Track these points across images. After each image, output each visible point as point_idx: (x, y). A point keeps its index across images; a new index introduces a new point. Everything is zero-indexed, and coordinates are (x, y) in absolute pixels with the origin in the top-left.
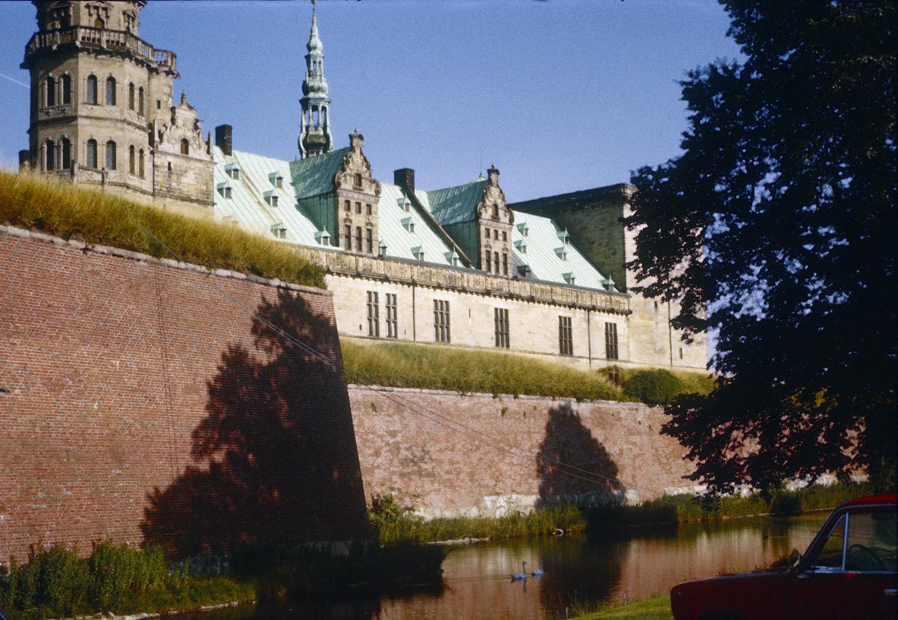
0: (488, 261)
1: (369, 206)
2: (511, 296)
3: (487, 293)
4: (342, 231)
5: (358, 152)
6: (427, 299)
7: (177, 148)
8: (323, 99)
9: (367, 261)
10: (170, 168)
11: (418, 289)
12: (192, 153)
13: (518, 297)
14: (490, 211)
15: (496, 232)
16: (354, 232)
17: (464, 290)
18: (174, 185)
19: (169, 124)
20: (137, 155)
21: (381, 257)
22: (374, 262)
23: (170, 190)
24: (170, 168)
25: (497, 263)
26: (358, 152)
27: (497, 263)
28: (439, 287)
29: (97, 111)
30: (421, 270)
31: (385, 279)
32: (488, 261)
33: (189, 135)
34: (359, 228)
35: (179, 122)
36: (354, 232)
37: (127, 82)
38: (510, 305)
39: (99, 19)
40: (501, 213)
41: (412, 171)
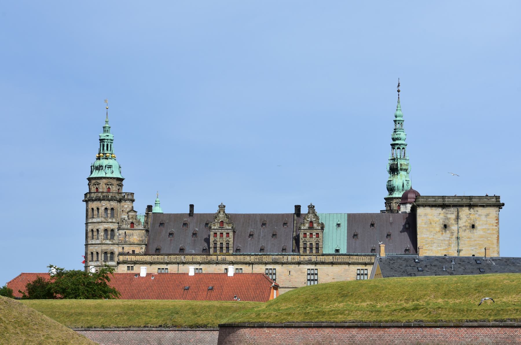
0: (305, 248)
1: (228, 234)
2: (316, 263)
3: (299, 263)
4: (212, 245)
5: (222, 212)
6: (261, 269)
7: (129, 226)
8: (397, 144)
9: (223, 257)
10: (125, 234)
11: (255, 266)
12: (135, 227)
13: (323, 263)
14: (307, 225)
15: (311, 234)
16: (218, 245)
17: (282, 264)
18: (127, 239)
19: (126, 218)
20: (109, 232)
21: (232, 255)
22: (227, 257)
23: (125, 242)
24: (125, 234)
25: (311, 248)
26: (222, 212)
27: (311, 248)
28: (266, 264)
29: (94, 220)
30: (256, 257)
31: (233, 263)
32: (305, 248)
33: (134, 221)
34: (221, 244)
35: (130, 216)
36: (218, 245)
37: (103, 208)
38: (318, 267)
39: (97, 188)
40: (315, 225)
41: (300, 206)
